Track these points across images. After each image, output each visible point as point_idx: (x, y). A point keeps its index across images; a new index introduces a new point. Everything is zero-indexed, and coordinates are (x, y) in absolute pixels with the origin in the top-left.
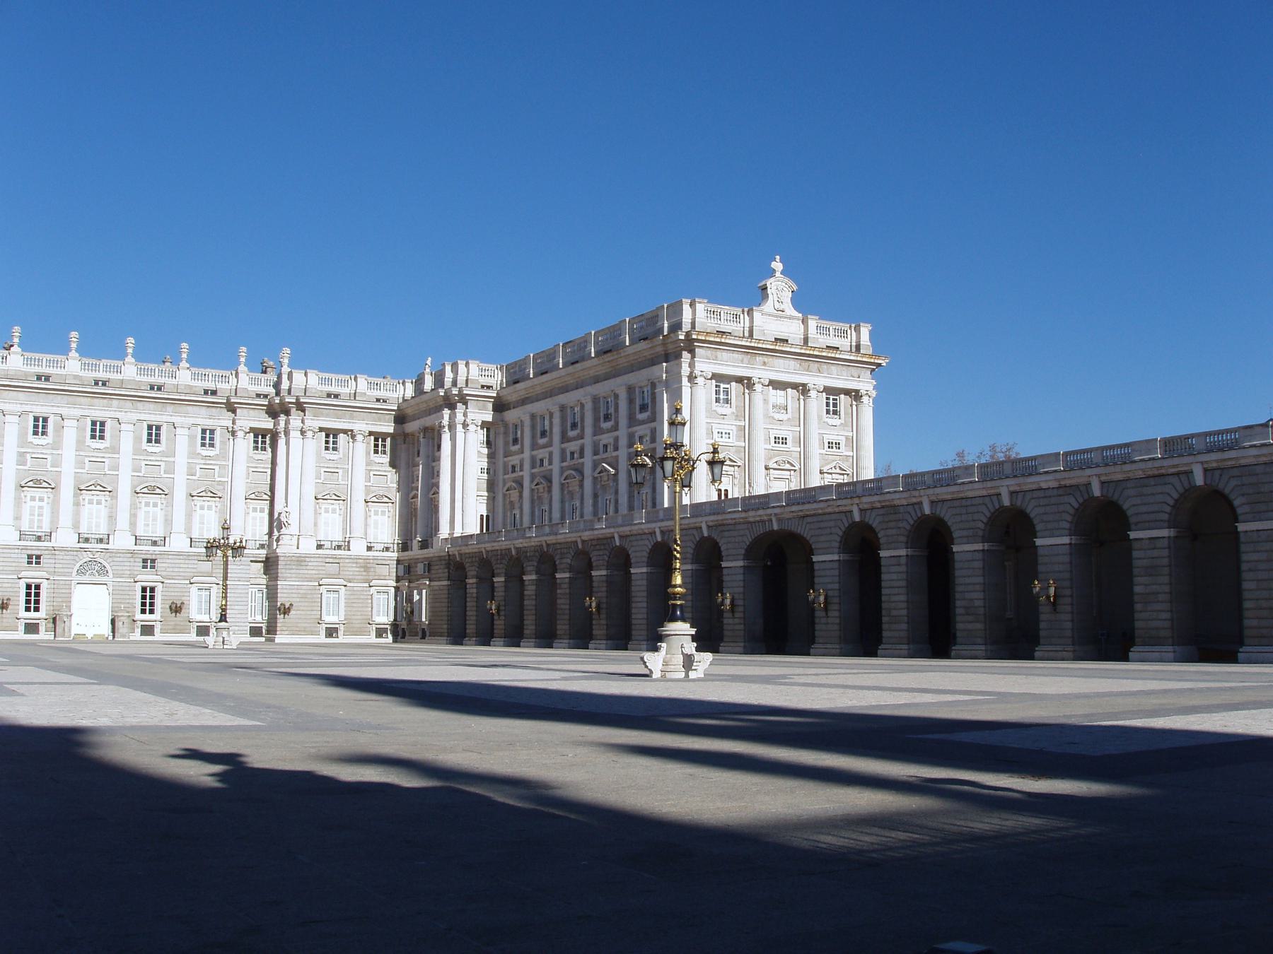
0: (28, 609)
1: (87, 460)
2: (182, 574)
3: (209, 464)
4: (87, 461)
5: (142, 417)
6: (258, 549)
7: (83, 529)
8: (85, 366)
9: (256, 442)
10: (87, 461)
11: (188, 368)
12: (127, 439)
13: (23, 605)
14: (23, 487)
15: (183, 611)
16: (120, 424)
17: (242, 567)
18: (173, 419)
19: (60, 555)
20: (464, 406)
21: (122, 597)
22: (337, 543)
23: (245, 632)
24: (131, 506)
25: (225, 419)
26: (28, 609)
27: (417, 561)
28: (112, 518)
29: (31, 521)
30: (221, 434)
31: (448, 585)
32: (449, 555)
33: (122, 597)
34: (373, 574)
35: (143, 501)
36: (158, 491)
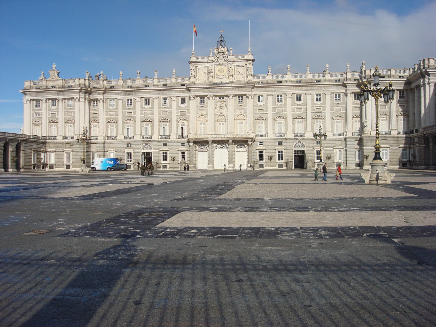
0: (279, 160)
1: (296, 108)
2: (331, 146)
3: (338, 106)
4: (296, 109)
5: (314, 92)
6: (358, 136)
7: (296, 132)
8: (293, 76)
9: (355, 97)
10: (296, 109)
11: (329, 73)
12: (309, 100)
13: (277, 158)
14: (275, 119)
15: (331, 158)
16: (306, 95)
17: (352, 142)
18: (324, 92)
19: (288, 141)
20: (428, 76)
21: (310, 154)
22: (386, 132)
23: (354, 166)
24: (311, 123)
25: (343, 90)
26: (279, 160)
27: (415, 137)
28: (306, 128)
29: (279, 130)
30: (342, 96)
31: (425, 146)
32: (424, 135)
33: (310, 154)
34: (400, 143)
35: (316, 121)
36: (321, 117)
